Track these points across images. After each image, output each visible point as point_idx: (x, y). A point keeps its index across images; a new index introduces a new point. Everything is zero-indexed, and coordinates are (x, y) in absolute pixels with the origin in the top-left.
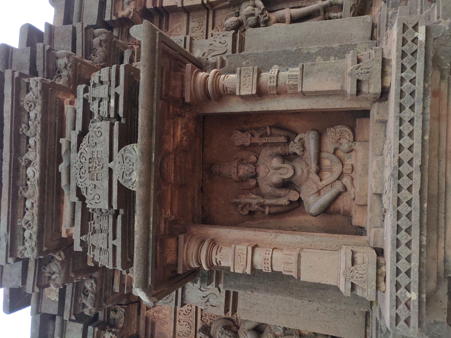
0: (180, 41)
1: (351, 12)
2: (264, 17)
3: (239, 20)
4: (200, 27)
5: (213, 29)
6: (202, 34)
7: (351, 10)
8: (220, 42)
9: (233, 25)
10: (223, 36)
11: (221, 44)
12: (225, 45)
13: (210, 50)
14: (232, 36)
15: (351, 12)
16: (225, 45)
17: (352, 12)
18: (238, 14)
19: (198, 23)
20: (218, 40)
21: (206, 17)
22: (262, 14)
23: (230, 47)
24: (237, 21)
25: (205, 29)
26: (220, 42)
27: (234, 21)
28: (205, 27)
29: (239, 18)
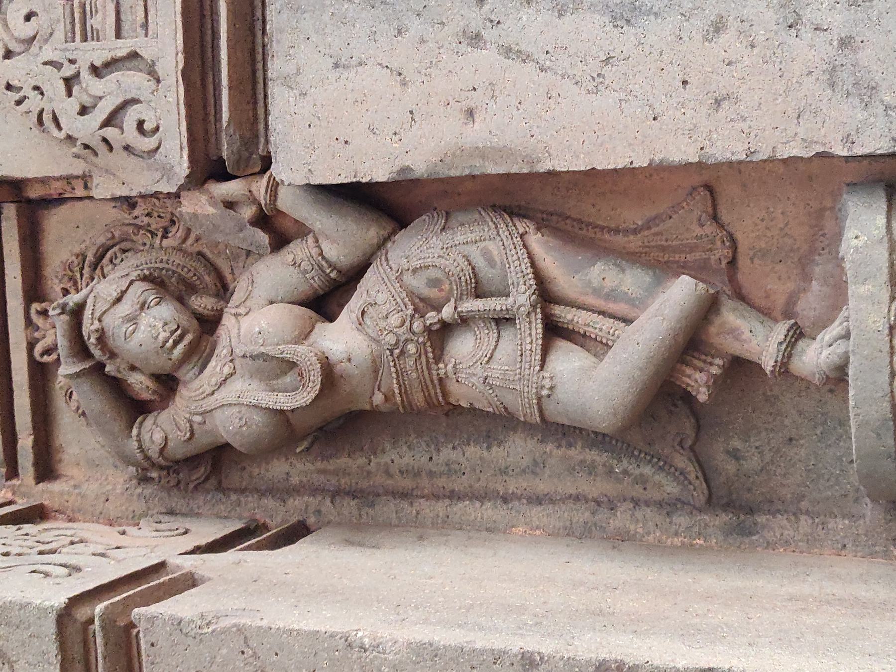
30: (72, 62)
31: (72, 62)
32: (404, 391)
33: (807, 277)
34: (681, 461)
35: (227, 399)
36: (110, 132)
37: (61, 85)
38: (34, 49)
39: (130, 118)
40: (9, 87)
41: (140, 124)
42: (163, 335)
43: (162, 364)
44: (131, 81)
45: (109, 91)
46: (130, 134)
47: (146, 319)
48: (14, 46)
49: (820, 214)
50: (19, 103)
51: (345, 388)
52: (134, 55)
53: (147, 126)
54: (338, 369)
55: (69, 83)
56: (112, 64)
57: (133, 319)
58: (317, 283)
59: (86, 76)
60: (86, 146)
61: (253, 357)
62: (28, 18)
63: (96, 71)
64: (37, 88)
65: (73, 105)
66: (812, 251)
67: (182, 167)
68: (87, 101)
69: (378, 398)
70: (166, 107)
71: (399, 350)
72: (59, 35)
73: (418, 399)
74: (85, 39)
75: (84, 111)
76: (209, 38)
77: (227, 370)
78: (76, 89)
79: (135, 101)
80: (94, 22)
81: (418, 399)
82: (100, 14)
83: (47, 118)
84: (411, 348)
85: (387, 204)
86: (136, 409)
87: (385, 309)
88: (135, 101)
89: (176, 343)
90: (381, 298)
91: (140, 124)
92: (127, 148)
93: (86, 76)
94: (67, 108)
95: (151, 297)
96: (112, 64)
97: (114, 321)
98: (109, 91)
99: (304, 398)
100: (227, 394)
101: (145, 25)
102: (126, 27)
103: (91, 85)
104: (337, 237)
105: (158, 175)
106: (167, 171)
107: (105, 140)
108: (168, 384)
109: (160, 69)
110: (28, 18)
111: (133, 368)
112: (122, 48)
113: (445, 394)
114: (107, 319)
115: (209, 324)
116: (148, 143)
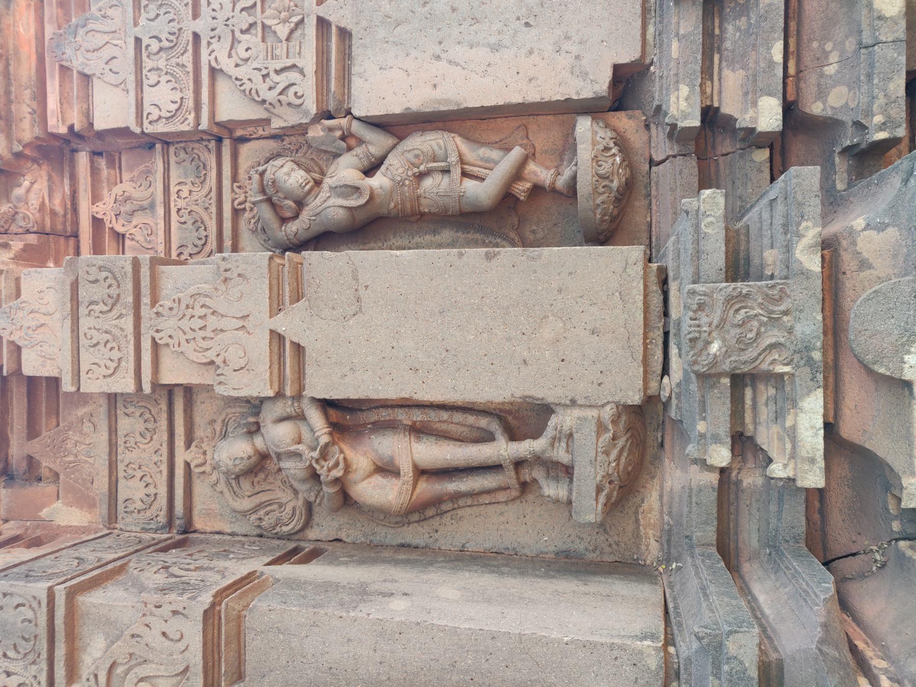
0: (35, 605)
1: (597, 500)
2: (329, 470)
3: (257, 452)
4: (148, 435)
5: (188, 446)
6: (156, 458)
7: (599, 489)
8: (164, 634)
9: (240, 467)
10: (175, 613)
11: (167, 643)
12: (181, 646)
13: (131, 655)
14: (200, 618)
15: (597, 500)
16: (181, 646)
17: (602, 499)
18: (254, 430)
19: (141, 420)
20: (158, 626)
21: (164, 407)
22: (324, 456)
23: (196, 657)
24: (249, 458)
25: (165, 445)
26: (164, 634)
27: (242, 458)
28: (165, 437)
29: (259, 442)
30: (266, 68)
31: (266, 68)
32: (403, 203)
33: (562, 160)
34: (512, 235)
35: (329, 207)
36: (282, 98)
37: (261, 78)
38: (249, 63)
39: (292, 90)
40: (237, 79)
41: (296, 93)
42: (301, 181)
43: (299, 193)
44: (293, 76)
45: (283, 80)
46: (291, 98)
47: (293, 174)
48: (240, 62)
49: (568, 135)
50: (241, 86)
51: (378, 200)
52: (294, 66)
53: (299, 94)
54: (376, 192)
55: (265, 77)
56: (284, 70)
57: (289, 174)
58: (366, 163)
59: (272, 74)
60: (270, 104)
61: (341, 187)
62: (247, 50)
63: (277, 72)
64: (249, 79)
65: (265, 86)
66: (564, 150)
67: (313, 110)
68: (272, 84)
69: (392, 205)
70: (307, 88)
71: (401, 184)
72: (261, 57)
73: (408, 206)
74: (272, 59)
75: (270, 89)
76: (325, 61)
77: (328, 195)
78: (267, 80)
79: (293, 84)
80: (278, 52)
81: (408, 206)
82: (279, 50)
83: (253, 92)
84: (407, 182)
85: (396, 126)
86: (284, 220)
87: (397, 166)
88: (293, 84)
89: (306, 184)
90: (395, 163)
91: (296, 93)
92: (289, 104)
93: (272, 74)
94: (263, 88)
95: (295, 166)
96: (284, 70)
97: (281, 174)
98: (283, 80)
99: (362, 201)
100: (331, 202)
101: (299, 54)
102: (290, 55)
103: (277, 78)
104: (377, 142)
105: (301, 116)
106: (306, 113)
107: (279, 101)
108: (300, 204)
109: (305, 71)
110: (247, 50)
111: (285, 198)
112: (289, 63)
113: (419, 205)
114: (277, 174)
115: (318, 183)
116: (299, 102)
